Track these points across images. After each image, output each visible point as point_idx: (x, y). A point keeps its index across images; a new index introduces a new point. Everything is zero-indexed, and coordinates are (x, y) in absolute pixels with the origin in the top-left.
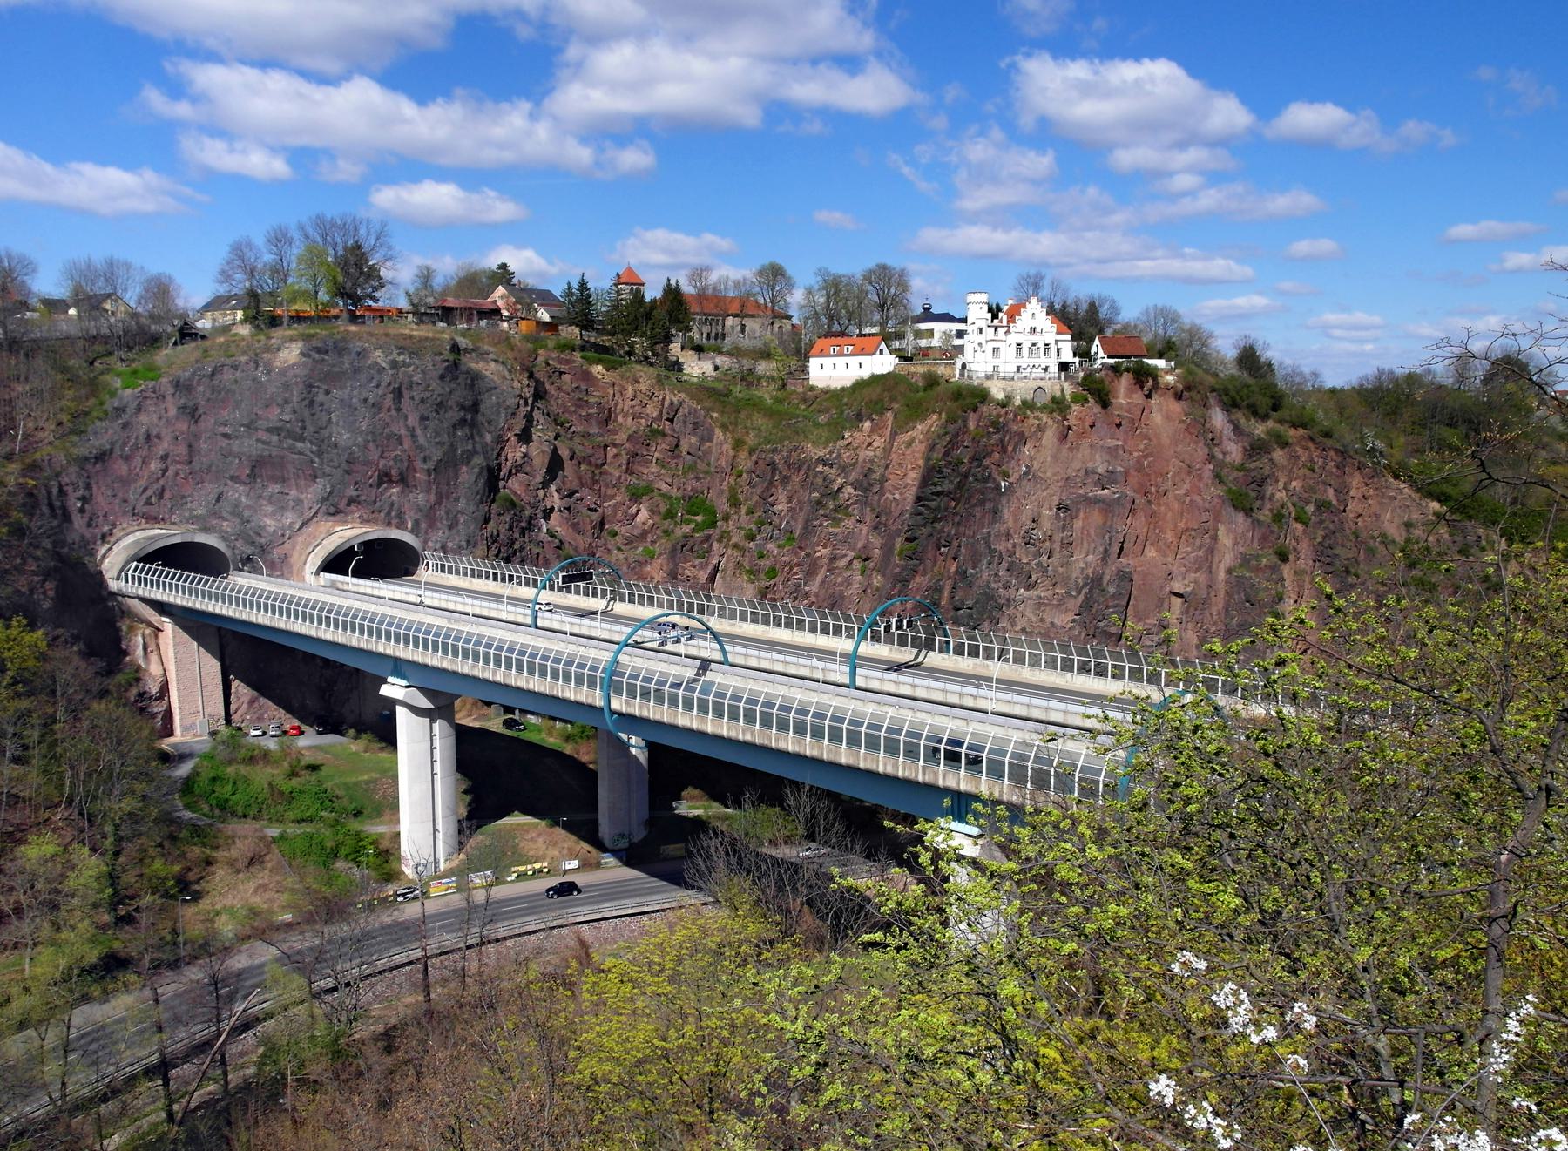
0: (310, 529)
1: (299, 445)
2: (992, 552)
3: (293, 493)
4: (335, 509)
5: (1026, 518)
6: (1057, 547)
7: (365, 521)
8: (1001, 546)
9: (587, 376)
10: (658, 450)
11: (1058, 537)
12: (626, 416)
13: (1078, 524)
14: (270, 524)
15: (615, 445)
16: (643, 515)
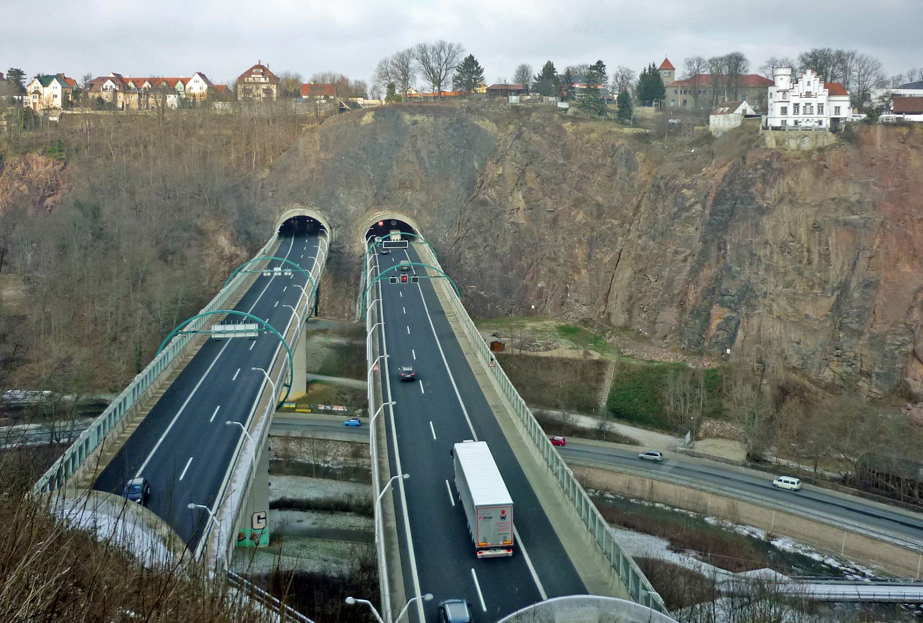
0: (368, 213)
1: (365, 166)
2: (753, 255)
3: (364, 191)
4: (379, 202)
5: (783, 233)
6: (815, 258)
7: (390, 210)
8: (761, 253)
9: (560, 129)
10: (599, 177)
11: (815, 249)
12: (582, 153)
13: (832, 241)
14: (352, 208)
15: (571, 172)
16: (580, 217)
